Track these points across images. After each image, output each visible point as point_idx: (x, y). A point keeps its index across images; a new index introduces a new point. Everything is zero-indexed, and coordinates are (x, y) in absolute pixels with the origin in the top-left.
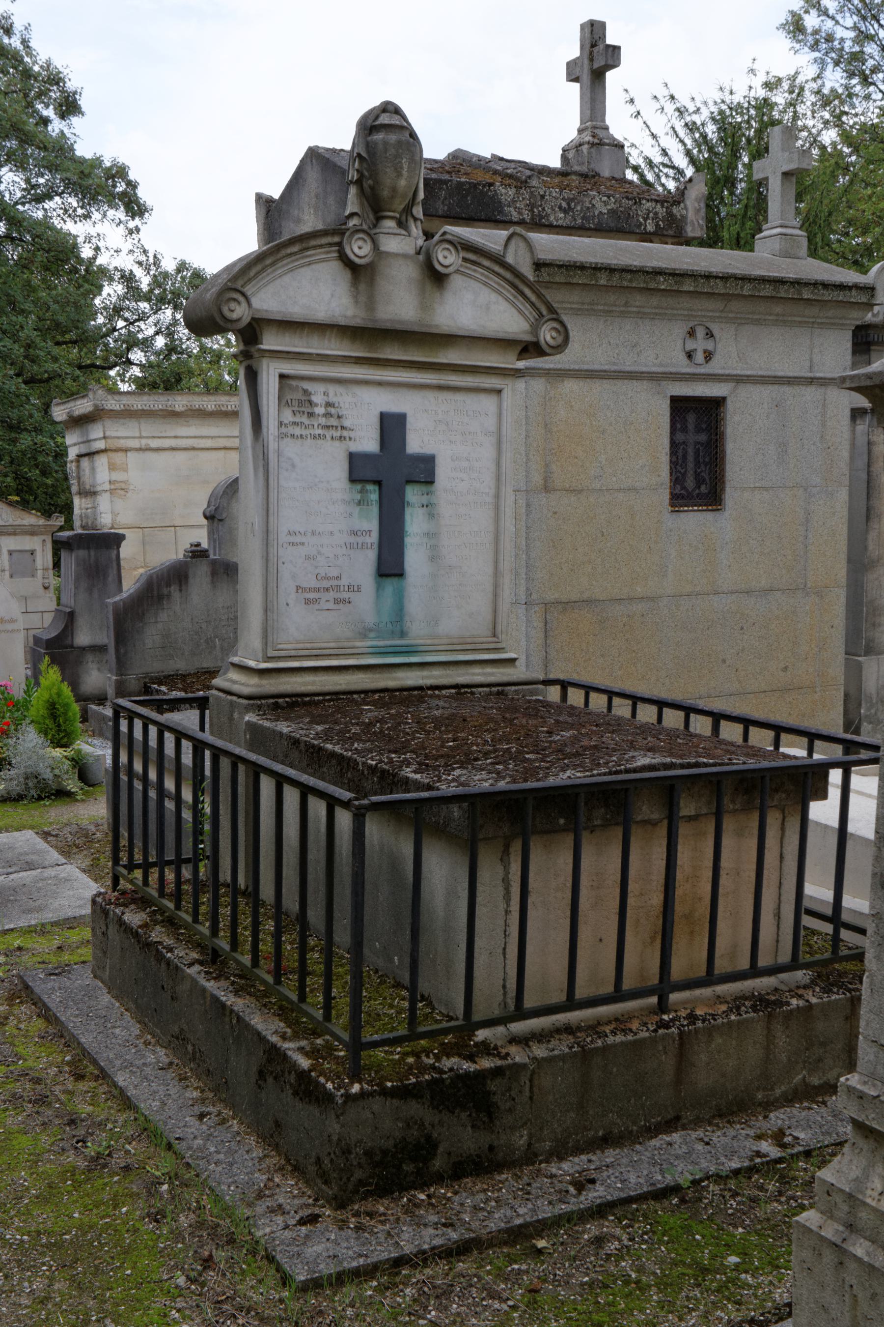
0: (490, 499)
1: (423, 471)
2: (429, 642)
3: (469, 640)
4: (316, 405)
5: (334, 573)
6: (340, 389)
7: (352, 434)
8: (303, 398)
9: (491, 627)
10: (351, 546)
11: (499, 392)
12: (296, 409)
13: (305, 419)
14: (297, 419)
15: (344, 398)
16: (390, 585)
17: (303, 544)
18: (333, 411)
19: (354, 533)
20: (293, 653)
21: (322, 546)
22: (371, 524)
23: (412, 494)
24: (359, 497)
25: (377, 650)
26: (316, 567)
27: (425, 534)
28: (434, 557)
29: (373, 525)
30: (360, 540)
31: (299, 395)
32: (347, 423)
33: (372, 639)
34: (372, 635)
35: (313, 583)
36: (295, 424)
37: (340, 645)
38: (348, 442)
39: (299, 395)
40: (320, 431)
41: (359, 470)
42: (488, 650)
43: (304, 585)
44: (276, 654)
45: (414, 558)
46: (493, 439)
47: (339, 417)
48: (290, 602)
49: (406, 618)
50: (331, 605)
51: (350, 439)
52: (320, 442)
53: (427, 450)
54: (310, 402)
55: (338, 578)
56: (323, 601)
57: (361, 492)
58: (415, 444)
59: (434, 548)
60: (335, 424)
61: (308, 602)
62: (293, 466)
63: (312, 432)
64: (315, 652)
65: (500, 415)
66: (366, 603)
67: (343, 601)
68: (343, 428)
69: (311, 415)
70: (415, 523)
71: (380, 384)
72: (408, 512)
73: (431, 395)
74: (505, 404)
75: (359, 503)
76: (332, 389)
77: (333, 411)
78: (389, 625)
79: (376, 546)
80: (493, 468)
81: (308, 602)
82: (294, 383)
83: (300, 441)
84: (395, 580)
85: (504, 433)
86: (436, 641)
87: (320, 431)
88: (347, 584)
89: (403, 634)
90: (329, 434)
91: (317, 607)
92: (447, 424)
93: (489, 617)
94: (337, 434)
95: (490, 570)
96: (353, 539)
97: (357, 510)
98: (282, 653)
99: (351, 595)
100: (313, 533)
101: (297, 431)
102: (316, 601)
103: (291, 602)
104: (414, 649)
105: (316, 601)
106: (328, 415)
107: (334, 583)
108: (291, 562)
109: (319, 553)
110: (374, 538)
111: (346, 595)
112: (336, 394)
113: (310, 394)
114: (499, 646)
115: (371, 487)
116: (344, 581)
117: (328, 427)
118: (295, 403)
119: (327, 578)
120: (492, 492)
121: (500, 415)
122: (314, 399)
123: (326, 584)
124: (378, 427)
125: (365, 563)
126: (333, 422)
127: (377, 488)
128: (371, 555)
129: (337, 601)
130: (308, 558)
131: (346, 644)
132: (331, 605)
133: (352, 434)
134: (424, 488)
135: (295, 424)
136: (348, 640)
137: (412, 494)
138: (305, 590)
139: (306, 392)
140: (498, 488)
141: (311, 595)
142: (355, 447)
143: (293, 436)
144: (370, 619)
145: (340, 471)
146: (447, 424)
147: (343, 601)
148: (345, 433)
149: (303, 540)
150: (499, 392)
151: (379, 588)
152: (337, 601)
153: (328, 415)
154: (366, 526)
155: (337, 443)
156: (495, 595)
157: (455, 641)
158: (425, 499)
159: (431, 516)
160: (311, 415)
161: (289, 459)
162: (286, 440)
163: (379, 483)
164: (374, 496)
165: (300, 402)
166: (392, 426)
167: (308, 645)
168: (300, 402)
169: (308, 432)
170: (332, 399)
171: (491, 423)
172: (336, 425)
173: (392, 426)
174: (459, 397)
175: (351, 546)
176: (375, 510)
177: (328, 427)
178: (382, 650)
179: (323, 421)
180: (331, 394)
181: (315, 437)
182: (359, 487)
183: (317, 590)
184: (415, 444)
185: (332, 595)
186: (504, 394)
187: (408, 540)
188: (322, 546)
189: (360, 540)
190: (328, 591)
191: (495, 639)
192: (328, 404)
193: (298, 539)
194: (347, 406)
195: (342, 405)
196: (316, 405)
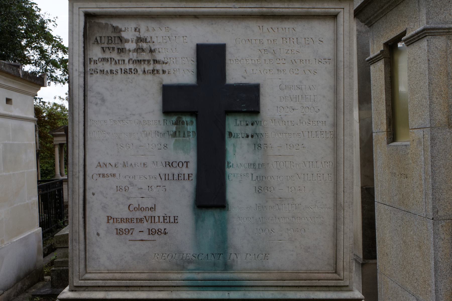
0: (327, 128)
1: (248, 100)
2: (255, 276)
3: (304, 276)
4: (127, 41)
5: (148, 203)
6: (152, 24)
7: (166, 67)
8: (113, 35)
9: (332, 261)
10: (166, 177)
11: (334, 17)
12: (105, 45)
13: (115, 55)
14: (107, 55)
15: (156, 33)
16: (210, 218)
17: (114, 175)
18: (144, 45)
19: (170, 164)
20: (100, 283)
21: (134, 177)
22: (188, 155)
23: (234, 125)
24: (174, 128)
25: (195, 283)
26: (128, 198)
27: (250, 165)
28: (262, 187)
29: (191, 156)
30: (176, 171)
31: (109, 33)
32: (159, 57)
33: (191, 271)
34: (191, 266)
35: (126, 214)
36: (104, 60)
37: (153, 276)
38: (161, 75)
39: (109, 33)
40: (132, 66)
41: (175, 101)
42: (328, 288)
43: (115, 215)
44: (82, 283)
45: (238, 188)
46: (330, 66)
47: (151, 51)
48: (101, 232)
49: (231, 251)
50: (145, 236)
51: (164, 72)
52: (130, 76)
53: (251, 80)
54: (121, 39)
55: (153, 209)
56: (135, 233)
57: (176, 123)
58: (235, 74)
59: (260, 178)
60: (147, 58)
61: (119, 232)
62: (103, 100)
63: (123, 67)
64: (124, 283)
65: (336, 40)
66: (184, 232)
67: (158, 232)
68: (156, 61)
69: (121, 51)
70: (238, 154)
71: (196, 16)
72: (230, 144)
73: (254, 26)
74: (341, 29)
75: (174, 135)
76: (143, 25)
77: (144, 45)
78: (211, 258)
79: (193, 177)
80: (330, 95)
81: (119, 232)
82: (103, 21)
83: (109, 77)
84: (216, 213)
85: (341, 58)
86: (264, 276)
87: (132, 66)
88: (161, 215)
89: (226, 267)
90: (140, 68)
91: (129, 237)
92: (274, 53)
93: (330, 251)
94: (151, 68)
95: (329, 202)
96: (168, 170)
97: (172, 142)
98: (89, 283)
99: (167, 226)
100: (124, 165)
101: (107, 67)
102: (128, 231)
103: (102, 232)
104: (238, 283)
105: (128, 231)
106: (139, 50)
107: (149, 213)
108: (101, 192)
109: (131, 184)
110: (192, 168)
111: (161, 226)
112: (147, 29)
113: (121, 31)
114: (341, 283)
115: (186, 119)
116: (159, 212)
117: (139, 62)
118: (105, 40)
119: (140, 209)
120: (330, 120)
121: (336, 40)
122: (124, 35)
123: (139, 214)
124: (195, 60)
125: (180, 197)
126: (145, 56)
127: (194, 120)
128: (189, 187)
129: (151, 232)
130: (119, 189)
131: (159, 276)
132: (145, 236)
133: (166, 67)
134: (249, 119)
135: (104, 60)
136: (165, 271)
137: (234, 125)
138: (116, 220)
139: (116, 29)
140: (336, 116)
141: (124, 226)
142: (169, 80)
143: (102, 71)
144: (189, 250)
145: (154, 102)
146: (274, 53)
147: (158, 232)
148: (158, 67)
149: (114, 171)
150: (334, 17)
151: (198, 219)
152: (151, 232)
153: (139, 50)
154: (182, 157)
155: (149, 77)
156: (336, 229)
157: (286, 276)
158: (249, 130)
159: (258, 146)
160: (121, 51)
161: (99, 93)
162: (95, 75)
163: (193, 113)
164: (191, 128)
165: (110, 40)
166: (211, 58)
167: (117, 276)
168: (110, 40)
169: (118, 67)
170: (143, 34)
171: (326, 50)
172: (148, 59)
173: (211, 58)
174: (288, 25)
175: (166, 177)
176: (192, 141)
177: (139, 62)
178: (200, 283)
179: (134, 56)
180: (143, 29)
181: (126, 72)
182: (174, 119)
183: (129, 220)
184: (235, 74)
185: (146, 225)
186: (340, 18)
187: (229, 171)
188: (134, 177)
189: (176, 171)
190: (142, 221)
191: (335, 276)
192: (139, 40)
193: (109, 171)
194: (160, 40)
195: (154, 39)
196: (127, 41)
